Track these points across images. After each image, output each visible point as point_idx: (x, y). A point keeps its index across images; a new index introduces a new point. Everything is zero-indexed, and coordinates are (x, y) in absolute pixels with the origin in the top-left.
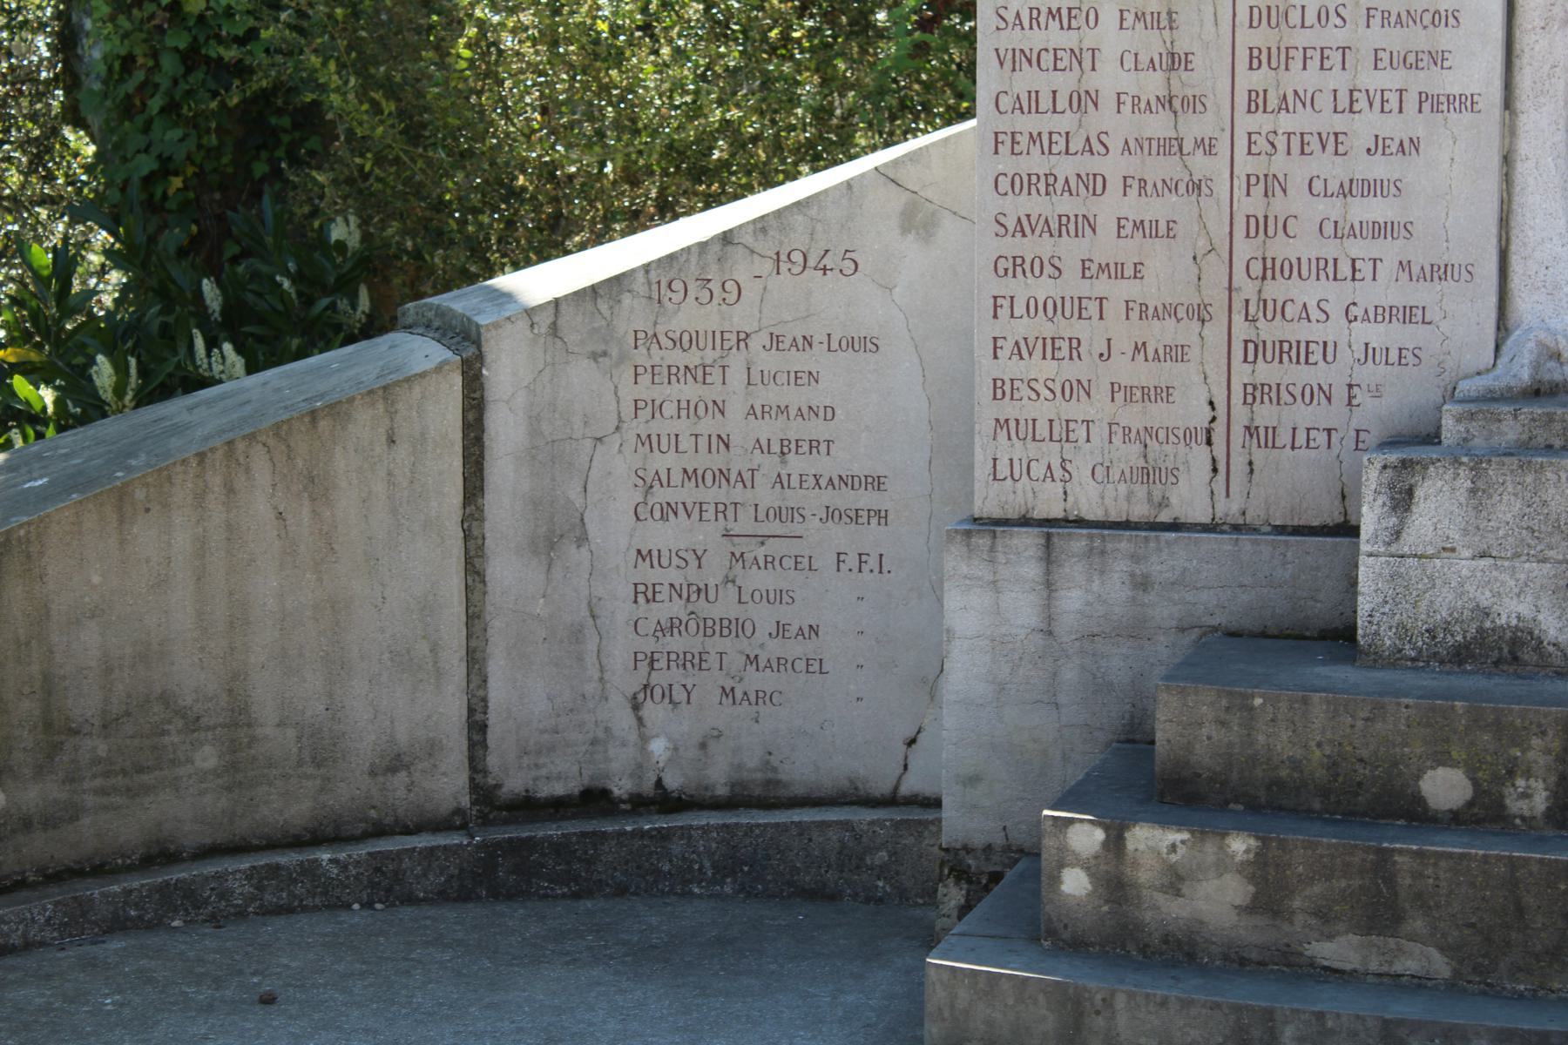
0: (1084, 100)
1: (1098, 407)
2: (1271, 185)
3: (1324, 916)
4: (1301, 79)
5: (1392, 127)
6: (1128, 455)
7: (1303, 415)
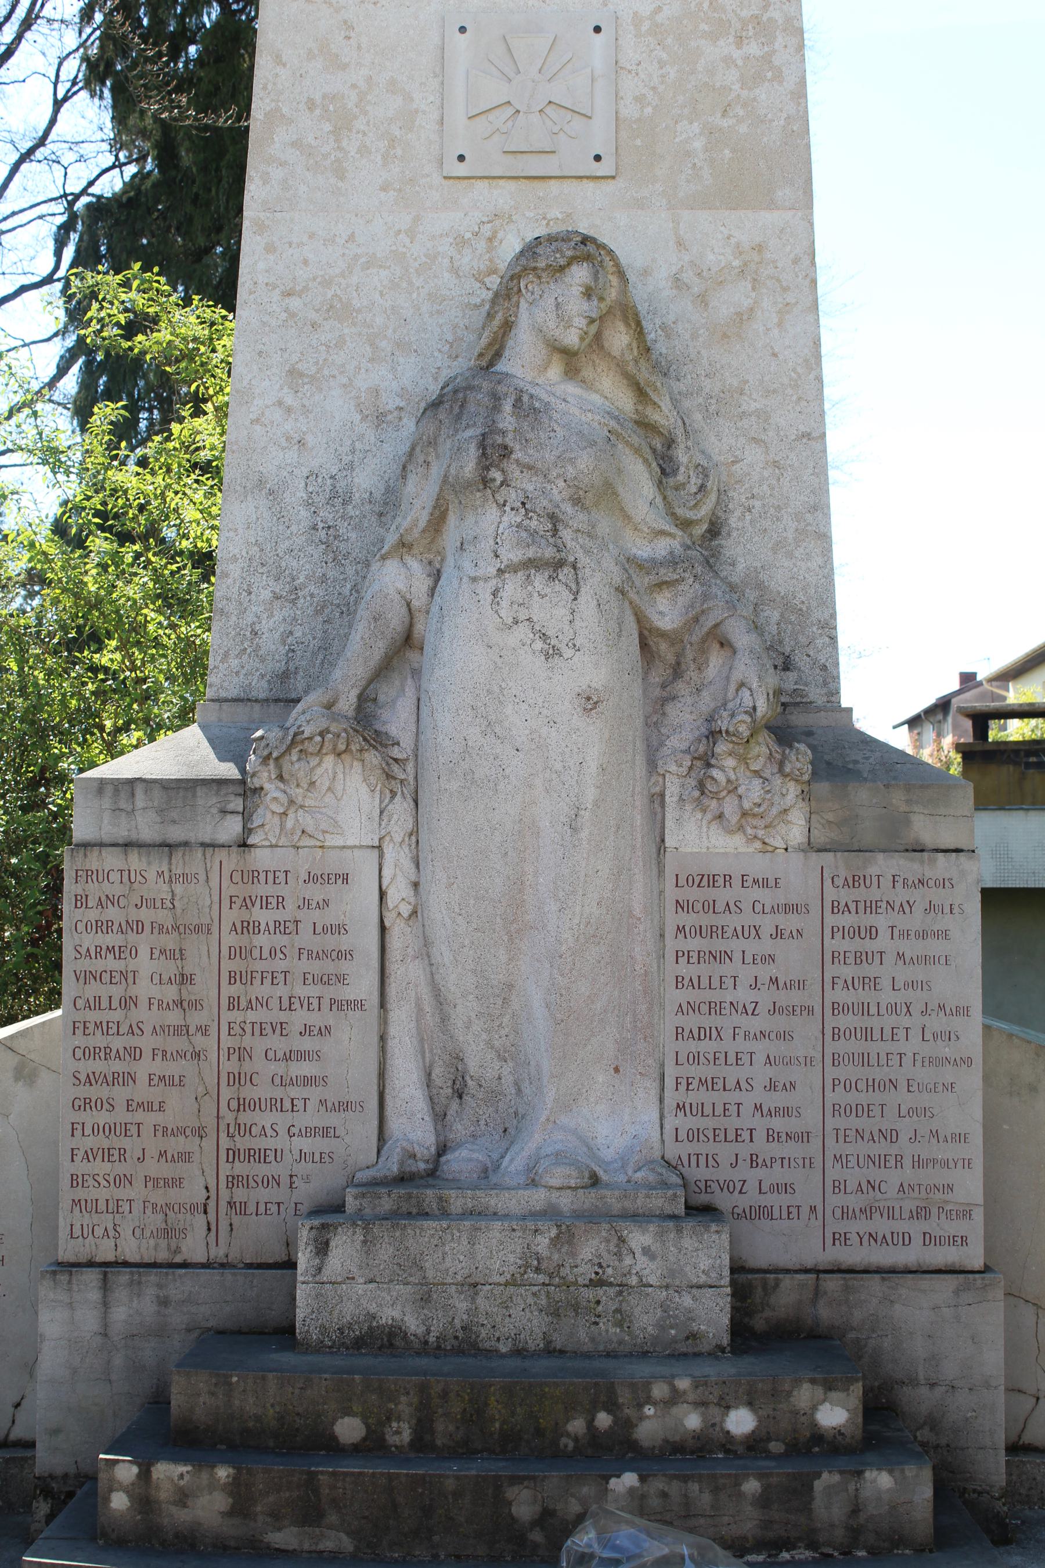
0: (128, 1002)
1: (136, 1192)
2: (242, 1054)
3: (276, 1517)
4: (261, 990)
5: (315, 1019)
6: (155, 1221)
7: (263, 1194)
